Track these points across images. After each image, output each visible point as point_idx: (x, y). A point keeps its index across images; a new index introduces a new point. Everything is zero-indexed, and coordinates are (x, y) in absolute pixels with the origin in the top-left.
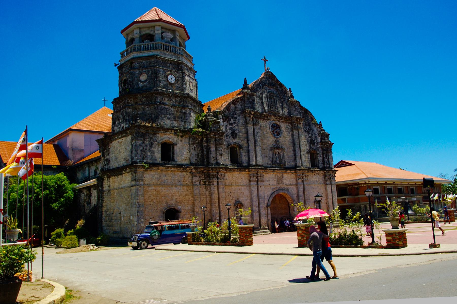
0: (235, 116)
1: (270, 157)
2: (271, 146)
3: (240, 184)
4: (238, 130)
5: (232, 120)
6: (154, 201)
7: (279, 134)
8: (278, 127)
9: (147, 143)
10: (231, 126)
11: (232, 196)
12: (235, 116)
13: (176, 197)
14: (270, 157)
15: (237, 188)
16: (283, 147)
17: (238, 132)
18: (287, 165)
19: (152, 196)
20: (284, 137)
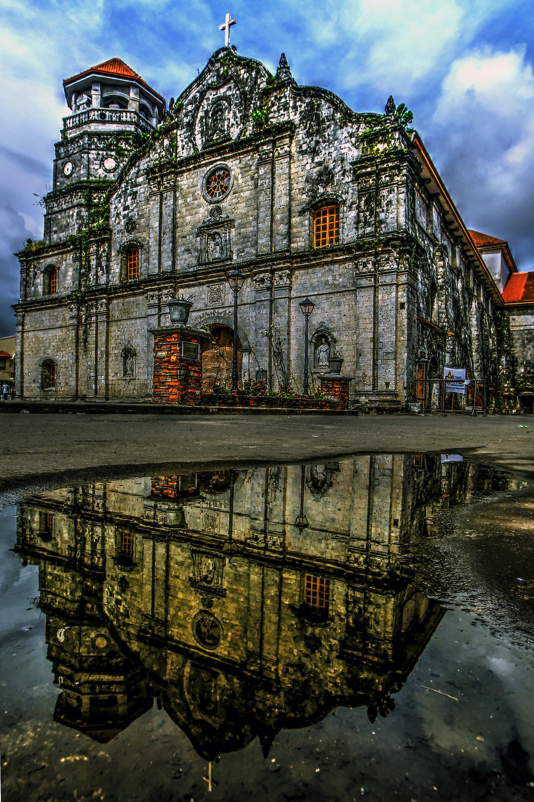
0: (135, 189)
1: (196, 250)
2: (200, 225)
3: (134, 315)
4: (138, 214)
5: (129, 198)
6: (33, 349)
7: (225, 190)
8: (227, 171)
9: (31, 274)
10: (126, 212)
11: (120, 337)
12: (135, 189)
13: (54, 344)
14: (196, 250)
15: (129, 322)
16: (232, 217)
17: (138, 219)
18: (235, 257)
19: (31, 344)
20: (234, 193)
